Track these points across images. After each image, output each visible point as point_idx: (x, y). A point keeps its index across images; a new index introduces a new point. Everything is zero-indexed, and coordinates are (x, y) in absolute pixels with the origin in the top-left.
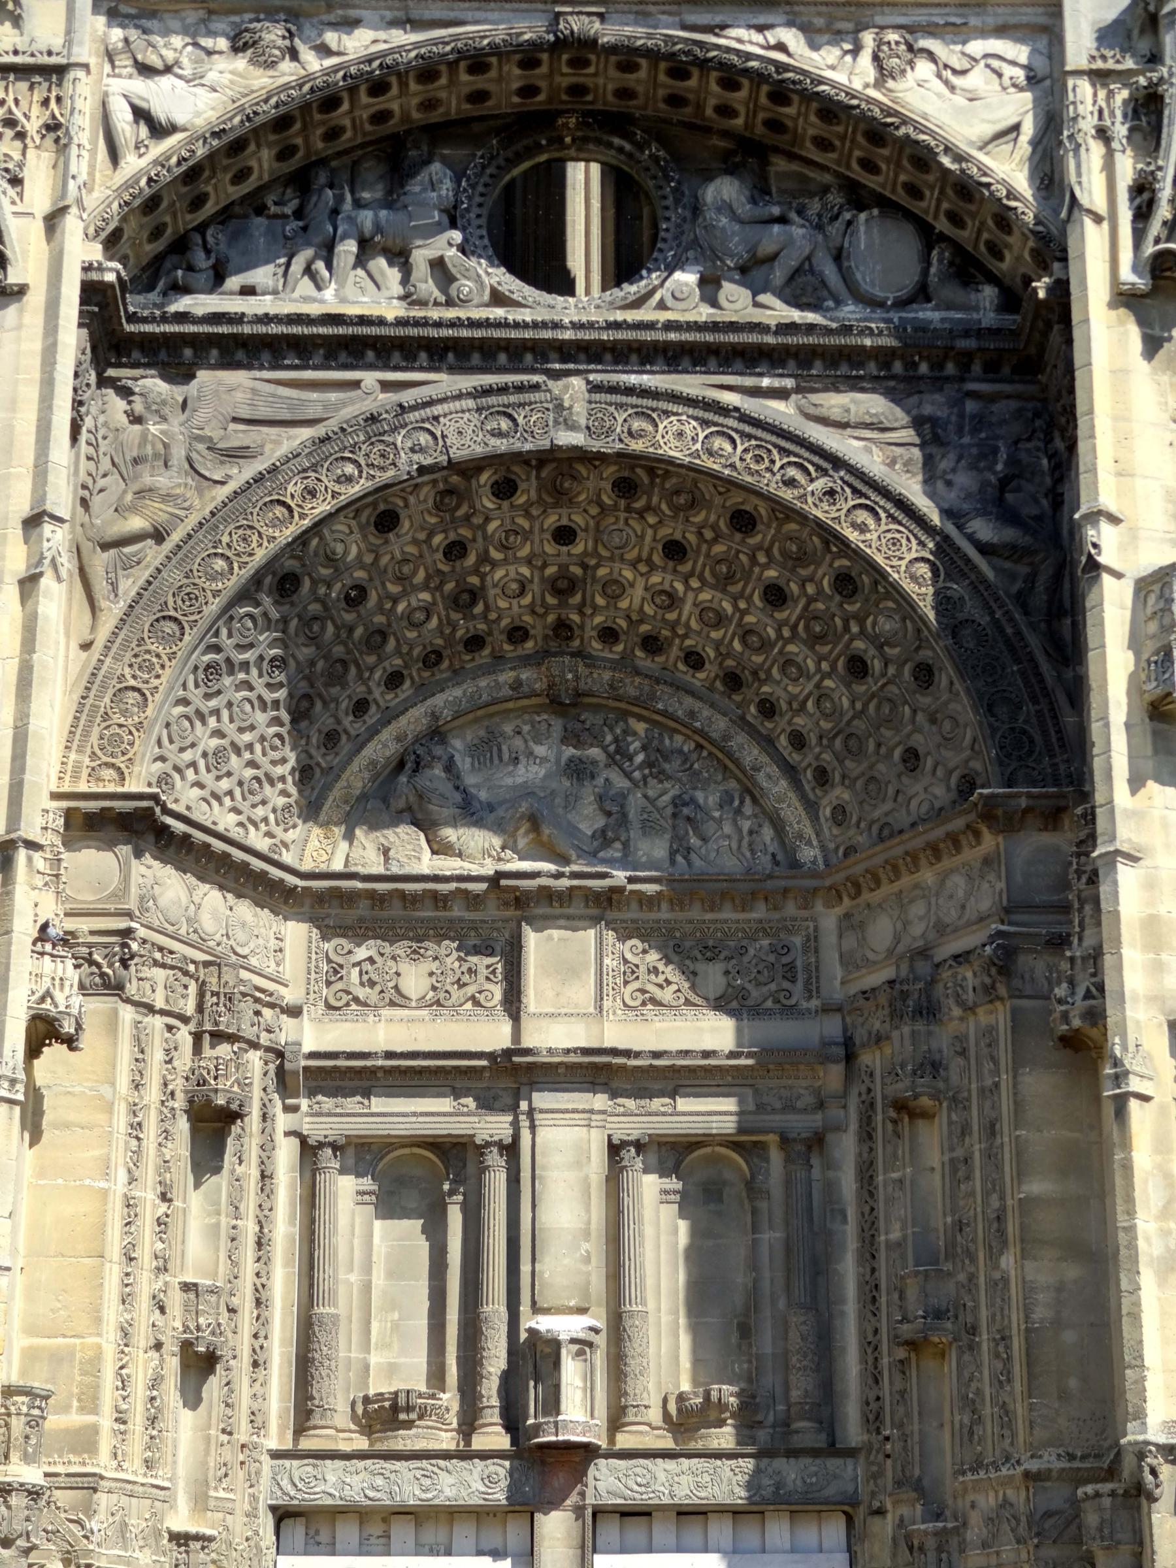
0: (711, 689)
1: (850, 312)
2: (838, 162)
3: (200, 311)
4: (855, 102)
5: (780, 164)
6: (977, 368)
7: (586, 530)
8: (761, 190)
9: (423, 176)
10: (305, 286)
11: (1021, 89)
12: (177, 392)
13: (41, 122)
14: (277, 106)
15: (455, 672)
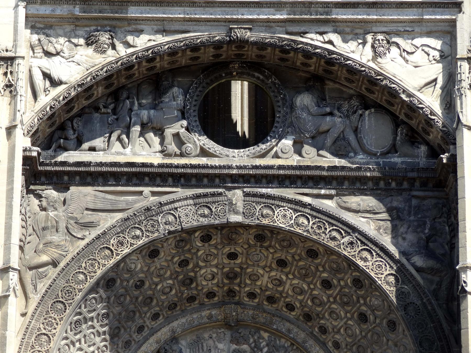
0: (298, 319)
1: (361, 157)
2: (356, 87)
3: (71, 160)
4: (363, 69)
6: (417, 184)
7: (242, 254)
8: (321, 100)
9: (169, 94)
10: (117, 146)
11: (438, 62)
12: (62, 196)
13: (4, 84)
14: (106, 72)
15: (182, 311)
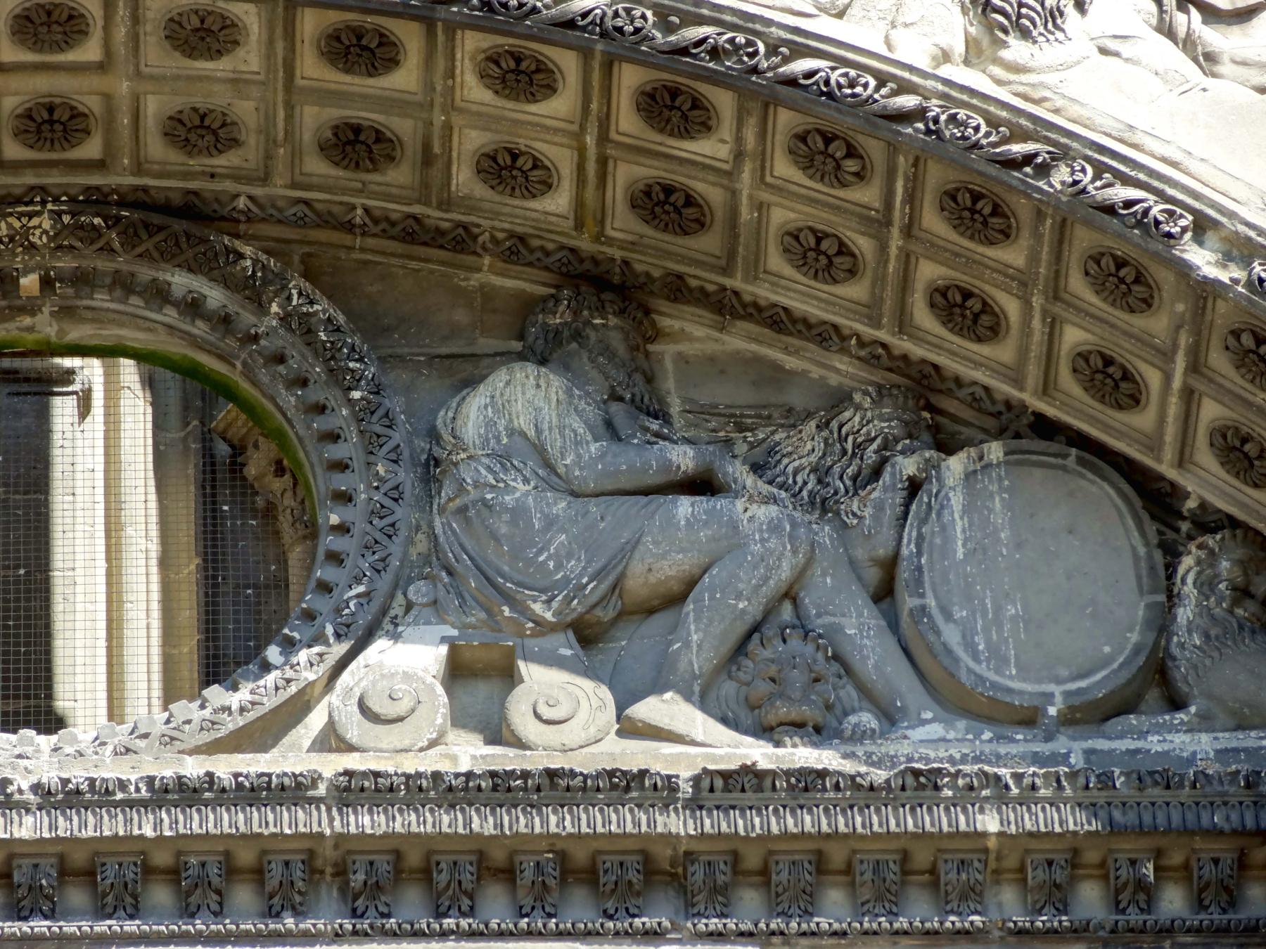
1: (930, 739)
4: (908, 101)
5: (689, 334)
8: (636, 402)
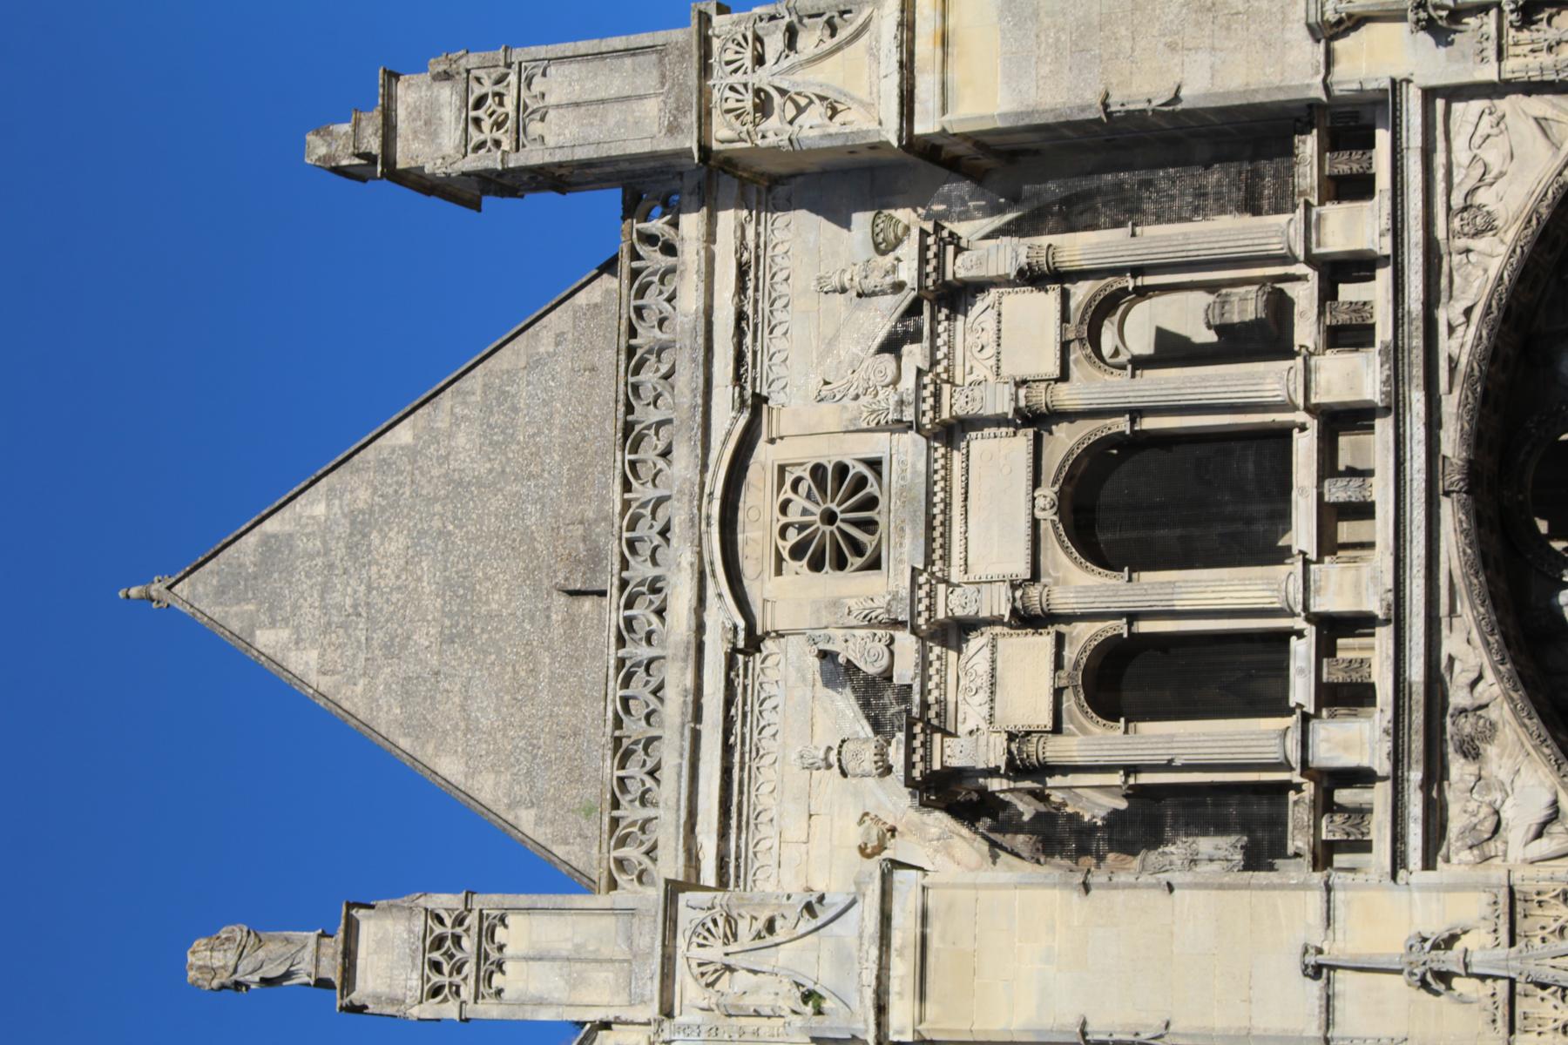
4: (1518, 250)
